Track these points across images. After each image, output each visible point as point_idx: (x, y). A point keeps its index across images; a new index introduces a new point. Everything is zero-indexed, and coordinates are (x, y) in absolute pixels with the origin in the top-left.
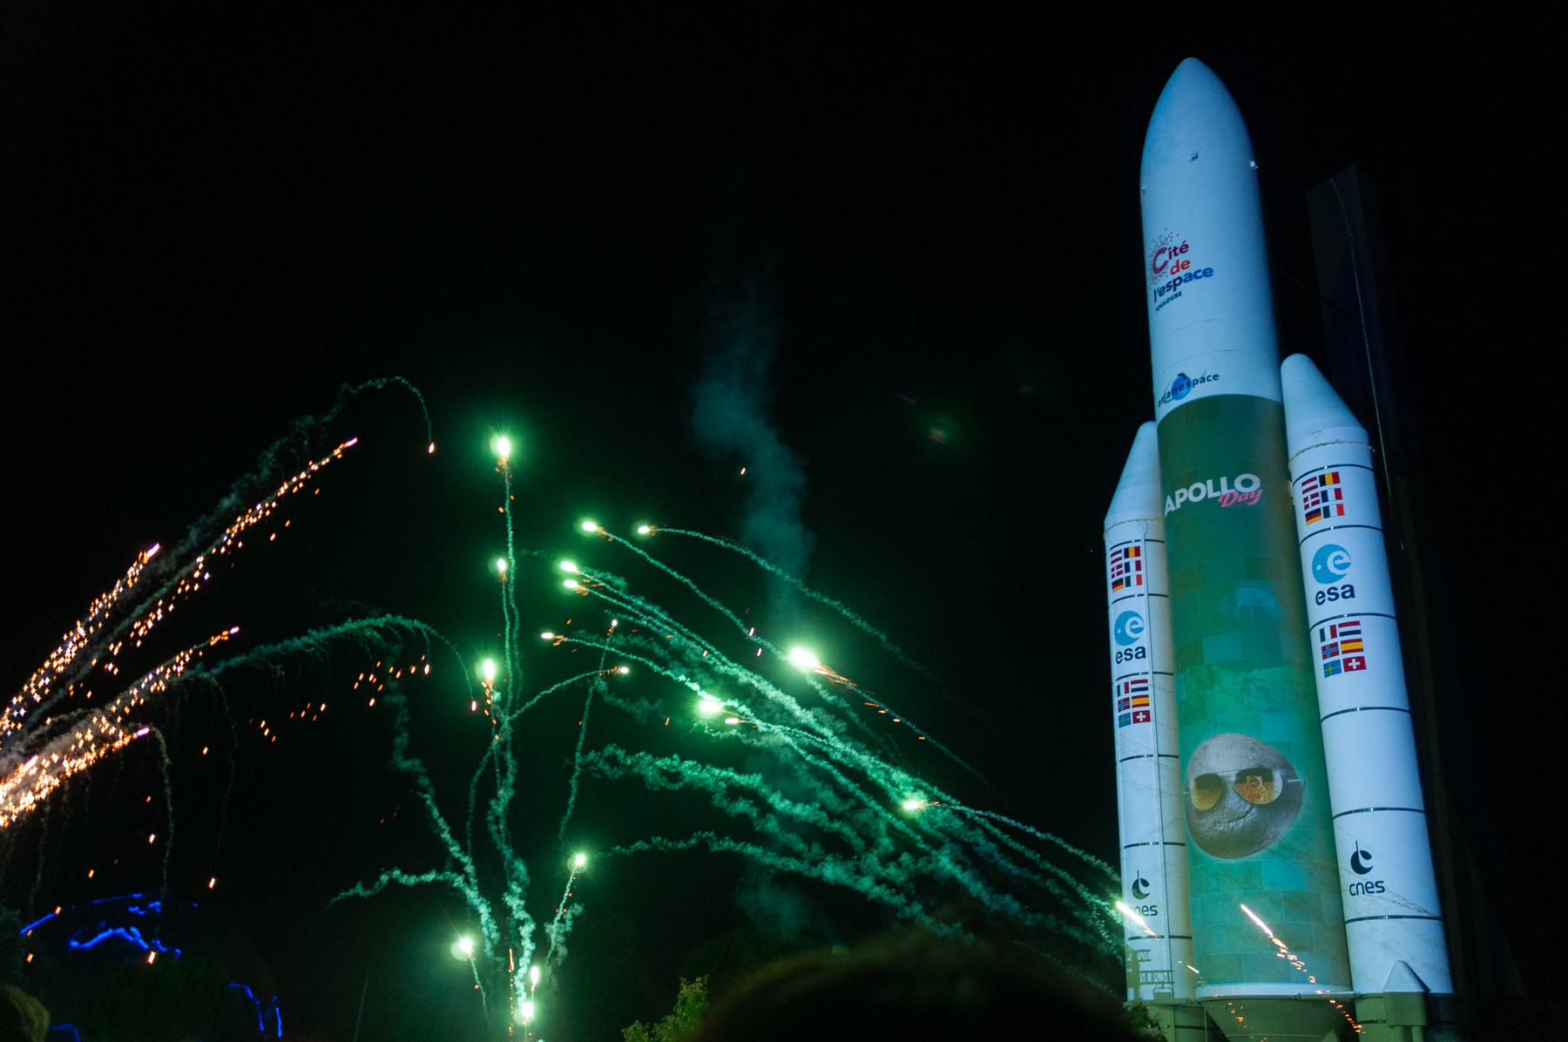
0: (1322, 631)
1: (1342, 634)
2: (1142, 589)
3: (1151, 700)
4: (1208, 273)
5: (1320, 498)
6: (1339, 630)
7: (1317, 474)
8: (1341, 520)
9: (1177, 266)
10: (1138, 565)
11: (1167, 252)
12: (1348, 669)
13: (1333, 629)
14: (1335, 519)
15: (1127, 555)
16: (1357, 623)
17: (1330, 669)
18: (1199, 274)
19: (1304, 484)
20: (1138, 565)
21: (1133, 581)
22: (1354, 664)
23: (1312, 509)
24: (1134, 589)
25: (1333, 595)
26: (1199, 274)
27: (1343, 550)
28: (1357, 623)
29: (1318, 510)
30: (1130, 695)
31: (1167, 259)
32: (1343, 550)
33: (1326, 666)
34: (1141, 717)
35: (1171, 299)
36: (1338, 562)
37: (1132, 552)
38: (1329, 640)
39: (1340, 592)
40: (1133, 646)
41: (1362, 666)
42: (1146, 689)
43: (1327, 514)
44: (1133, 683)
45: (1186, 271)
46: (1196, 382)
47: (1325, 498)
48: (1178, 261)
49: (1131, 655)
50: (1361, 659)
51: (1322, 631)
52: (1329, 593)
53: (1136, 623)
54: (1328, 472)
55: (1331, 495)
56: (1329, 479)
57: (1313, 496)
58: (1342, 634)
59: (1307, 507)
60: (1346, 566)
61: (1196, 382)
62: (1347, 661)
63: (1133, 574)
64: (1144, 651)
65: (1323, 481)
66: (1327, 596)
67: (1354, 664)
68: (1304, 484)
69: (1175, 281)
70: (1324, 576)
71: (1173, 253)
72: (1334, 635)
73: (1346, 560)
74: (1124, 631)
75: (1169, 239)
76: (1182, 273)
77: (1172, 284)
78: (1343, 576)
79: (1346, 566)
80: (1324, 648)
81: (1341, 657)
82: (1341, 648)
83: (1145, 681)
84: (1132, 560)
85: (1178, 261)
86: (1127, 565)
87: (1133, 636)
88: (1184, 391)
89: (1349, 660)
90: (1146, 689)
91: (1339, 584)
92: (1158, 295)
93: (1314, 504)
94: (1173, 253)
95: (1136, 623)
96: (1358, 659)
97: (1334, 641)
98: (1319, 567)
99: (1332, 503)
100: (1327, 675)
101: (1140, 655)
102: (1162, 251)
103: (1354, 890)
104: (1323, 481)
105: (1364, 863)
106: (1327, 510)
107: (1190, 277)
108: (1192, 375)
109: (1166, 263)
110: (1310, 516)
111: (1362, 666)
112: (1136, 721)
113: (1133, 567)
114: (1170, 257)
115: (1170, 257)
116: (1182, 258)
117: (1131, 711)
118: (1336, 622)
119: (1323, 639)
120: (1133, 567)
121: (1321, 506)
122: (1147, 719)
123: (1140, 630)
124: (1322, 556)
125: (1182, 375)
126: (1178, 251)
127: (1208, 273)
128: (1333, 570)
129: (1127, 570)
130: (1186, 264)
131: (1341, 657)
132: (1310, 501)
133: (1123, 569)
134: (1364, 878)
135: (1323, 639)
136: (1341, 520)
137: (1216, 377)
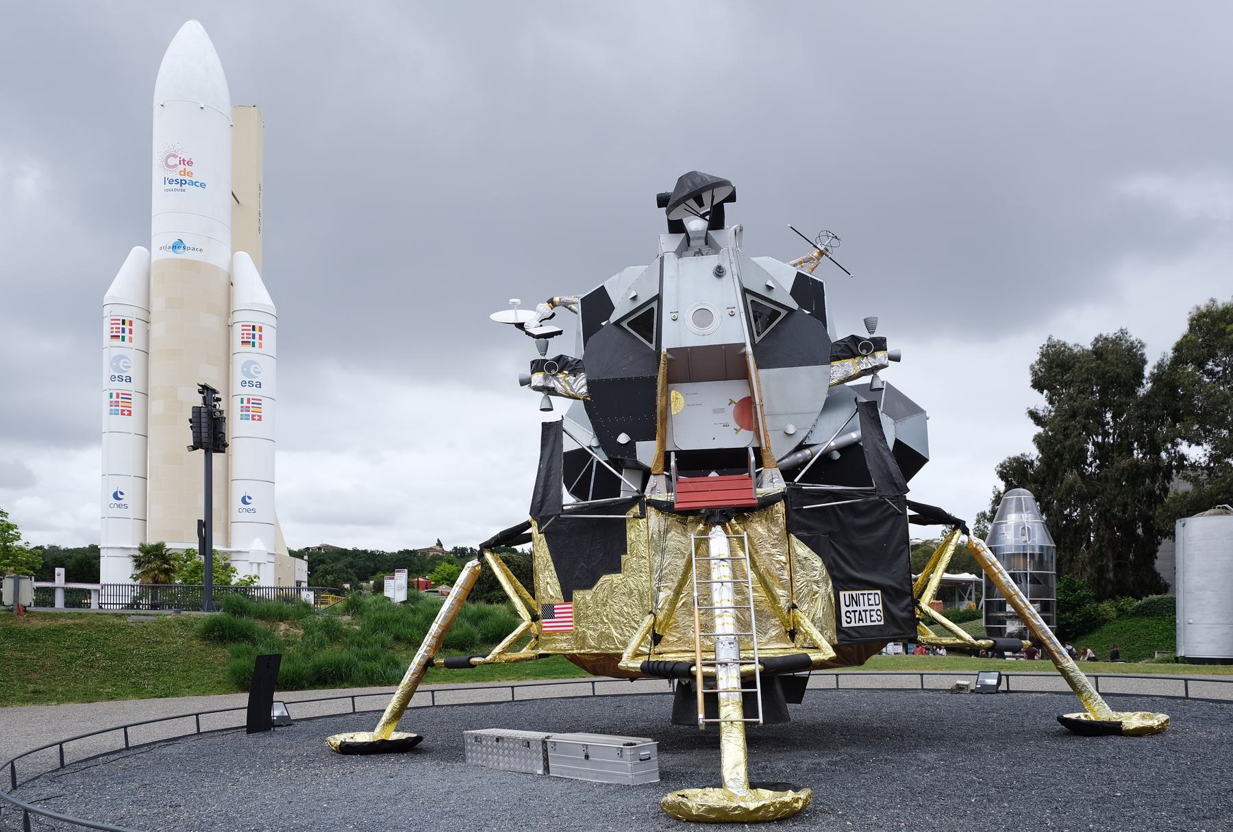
0: (242, 400)
1: (252, 403)
3: (132, 405)
4: (203, 185)
5: (251, 336)
7: (252, 324)
9: (185, 172)
12: (253, 419)
16: (260, 400)
18: (197, 184)
19: (243, 326)
21: (127, 339)
23: (245, 340)
25: (251, 384)
26: (197, 184)
27: (258, 364)
28: (260, 400)
29: (249, 342)
31: (178, 163)
33: (242, 415)
34: (126, 413)
35: (175, 190)
39: (254, 384)
41: (260, 419)
42: (130, 399)
43: (253, 346)
44: (122, 394)
47: (254, 338)
48: (185, 169)
49: (123, 380)
50: (260, 416)
51: (242, 400)
52: (249, 382)
53: (126, 362)
54: (257, 326)
55: (257, 337)
56: (257, 329)
57: (247, 334)
58: (252, 403)
59: (243, 338)
60: (259, 373)
62: (253, 416)
64: (130, 379)
65: (254, 329)
66: (248, 384)
67: (256, 418)
68: (243, 326)
69: (181, 180)
70: (247, 374)
71: (182, 162)
72: (249, 402)
76: (187, 178)
77: (179, 181)
78: (255, 377)
79: (259, 373)
80: (242, 407)
81: (251, 413)
82: (251, 409)
85: (185, 169)
87: (126, 369)
89: (255, 416)
90: (130, 399)
91: (255, 381)
92: (167, 182)
93: (247, 338)
94: (182, 162)
95: (126, 362)
96: (258, 416)
97: (248, 405)
98: (245, 369)
99: (257, 340)
100: (241, 419)
102: (176, 157)
103: (241, 510)
104: (254, 329)
105: (247, 500)
106: (254, 343)
107: (192, 183)
109: (176, 165)
111: (260, 420)
116: (188, 168)
119: (242, 402)
121: (251, 340)
123: (129, 367)
124: (248, 364)
126: (186, 163)
127: (203, 185)
130: (190, 174)
131: (251, 413)
132: (245, 336)
133: (121, 330)
135: (242, 402)
136: (259, 350)
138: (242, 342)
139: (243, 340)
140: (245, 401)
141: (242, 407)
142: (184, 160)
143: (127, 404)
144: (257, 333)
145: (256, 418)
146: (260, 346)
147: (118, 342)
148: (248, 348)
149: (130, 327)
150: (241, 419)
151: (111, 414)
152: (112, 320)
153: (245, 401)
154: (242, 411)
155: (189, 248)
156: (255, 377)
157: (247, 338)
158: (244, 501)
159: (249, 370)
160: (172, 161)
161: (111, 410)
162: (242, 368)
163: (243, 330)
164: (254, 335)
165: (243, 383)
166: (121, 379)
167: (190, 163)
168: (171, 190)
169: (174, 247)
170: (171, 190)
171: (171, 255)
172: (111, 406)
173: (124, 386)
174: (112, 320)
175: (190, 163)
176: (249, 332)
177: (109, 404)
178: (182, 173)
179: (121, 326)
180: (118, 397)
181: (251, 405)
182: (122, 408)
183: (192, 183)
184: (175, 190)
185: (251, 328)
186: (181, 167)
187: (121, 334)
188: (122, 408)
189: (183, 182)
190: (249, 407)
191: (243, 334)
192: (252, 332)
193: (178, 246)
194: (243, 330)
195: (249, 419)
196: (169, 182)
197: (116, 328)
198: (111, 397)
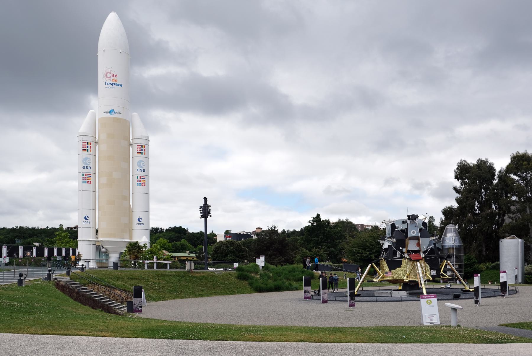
0: (138, 177)
2: (91, 153)
3: (92, 179)
4: (121, 85)
5: (141, 150)
7: (141, 145)
10: (91, 148)
11: (111, 74)
14: (143, 155)
15: (88, 144)
16: (145, 177)
17: (139, 184)
18: (119, 85)
19: (137, 145)
24: (89, 152)
26: (119, 85)
28: (145, 177)
29: (140, 152)
32: (144, 162)
33: (137, 183)
35: (110, 88)
36: (143, 164)
37: (89, 144)
38: (139, 179)
41: (145, 185)
42: (91, 176)
44: (88, 174)
45: (117, 83)
47: (142, 150)
50: (145, 184)
51: (138, 177)
53: (89, 161)
54: (143, 145)
55: (143, 150)
57: (139, 149)
60: (144, 165)
64: (91, 168)
65: (142, 147)
68: (137, 145)
69: (113, 83)
70: (139, 166)
71: (113, 76)
73: (144, 164)
75: (112, 71)
76: (115, 82)
77: (112, 84)
78: (143, 167)
79: (144, 165)
80: (137, 180)
81: (141, 183)
83: (91, 175)
84: (89, 146)
89: (143, 184)
91: (143, 169)
92: (107, 84)
93: (140, 151)
95: (89, 161)
96: (145, 184)
97: (140, 179)
99: (143, 152)
100: (137, 185)
101: (90, 168)
102: (110, 73)
103: (138, 224)
104: (142, 147)
105: (140, 220)
107: (118, 85)
109: (110, 77)
114: (112, 76)
115: (112, 76)
116: (115, 78)
118: (141, 176)
119: (138, 178)
121: (141, 152)
122: (91, 183)
126: (114, 76)
127: (121, 85)
128: (142, 165)
130: (116, 81)
132: (139, 150)
133: (87, 147)
135: (138, 178)
138: (137, 152)
139: (138, 151)
140: (139, 177)
141: (137, 180)
142: (114, 75)
143: (89, 179)
144: (143, 148)
145: (143, 185)
146: (145, 154)
147: (86, 152)
148: (140, 155)
149: (90, 146)
150: (137, 185)
151: (83, 183)
152: (83, 142)
153: (139, 177)
154: (137, 182)
155: (116, 113)
156: (143, 167)
157: (140, 151)
159: (140, 164)
160: (109, 75)
161: (83, 181)
163: (137, 147)
165: (138, 170)
166: (87, 168)
167: (116, 76)
168: (108, 88)
169: (110, 112)
170: (108, 88)
171: (109, 115)
172: (83, 179)
173: (88, 171)
174: (83, 142)
175: (116, 76)
176: (140, 148)
177: (82, 178)
178: (113, 80)
179: (87, 145)
180: (86, 175)
181: (141, 179)
182: (88, 180)
183: (118, 85)
184: (110, 88)
185: (141, 146)
186: (113, 78)
188: (88, 180)
189: (114, 84)
190: (140, 180)
191: (138, 149)
192: (141, 148)
193: (112, 112)
194: (137, 147)
196: (108, 84)
197: (85, 146)
198: (83, 175)
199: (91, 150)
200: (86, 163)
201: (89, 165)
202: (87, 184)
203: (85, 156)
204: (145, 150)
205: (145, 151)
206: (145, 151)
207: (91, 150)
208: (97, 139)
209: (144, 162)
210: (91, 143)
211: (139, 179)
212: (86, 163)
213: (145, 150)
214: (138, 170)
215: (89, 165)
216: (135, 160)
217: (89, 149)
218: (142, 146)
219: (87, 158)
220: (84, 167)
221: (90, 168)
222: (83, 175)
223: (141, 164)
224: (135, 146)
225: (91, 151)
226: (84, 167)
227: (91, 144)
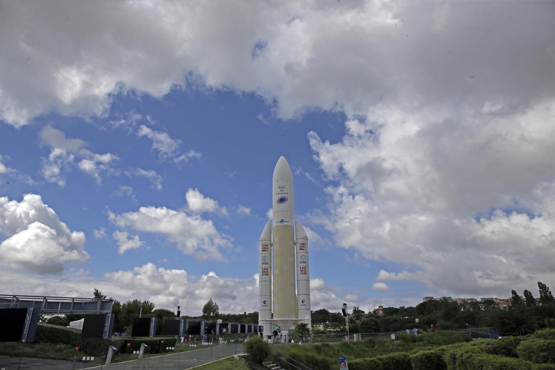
2: (268, 252)
6: (303, 268)
7: (302, 243)
8: (305, 251)
10: (268, 249)
13: (303, 267)
15: (266, 246)
20: (268, 249)
21: (267, 251)
22: (305, 273)
25: (303, 262)
30: (265, 270)
37: (267, 246)
38: (302, 269)
40: (266, 262)
46: (285, 222)
47: (303, 247)
54: (304, 243)
60: (305, 258)
61: (285, 222)
62: (304, 273)
63: (267, 249)
65: (303, 245)
67: (305, 273)
70: (302, 259)
72: (303, 268)
74: (264, 259)
79: (305, 258)
84: (267, 247)
86: (266, 248)
88: (283, 222)
91: (304, 261)
96: (306, 273)
98: (301, 258)
99: (304, 248)
100: (301, 274)
104: (303, 244)
105: (304, 301)
106: (303, 249)
108: (285, 220)
110: (300, 249)
111: (306, 274)
112: (266, 275)
113: (267, 248)
117: (265, 273)
118: (303, 267)
120: (267, 248)
121: (302, 248)
122: (268, 275)
125: (283, 219)
129: (266, 249)
134: (303, 304)
137: (288, 222)
140: (302, 268)
144: (304, 246)
146: (305, 250)
147: (264, 252)
151: (263, 275)
153: (302, 268)
158: (302, 302)
159: (302, 258)
162: (300, 258)
164: (303, 247)
169: (281, 222)
173: (266, 266)
177: (262, 272)
181: (303, 269)
185: (302, 244)
187: (265, 249)
192: (303, 246)
195: (302, 274)
198: (263, 269)
199: (268, 250)
200: (264, 260)
201: (266, 261)
202: (265, 276)
203: (264, 255)
204: (305, 247)
205: (305, 247)
206: (305, 247)
207: (268, 250)
208: (272, 242)
209: (305, 256)
210: (268, 245)
211: (302, 269)
212: (265, 260)
213: (305, 247)
214: (301, 262)
215: (266, 261)
216: (299, 254)
217: (267, 249)
218: (303, 244)
219: (265, 257)
220: (263, 264)
221: (267, 264)
222: (263, 269)
223: (303, 257)
224: (298, 245)
225: (268, 251)
226: (263, 264)
227: (268, 246)
